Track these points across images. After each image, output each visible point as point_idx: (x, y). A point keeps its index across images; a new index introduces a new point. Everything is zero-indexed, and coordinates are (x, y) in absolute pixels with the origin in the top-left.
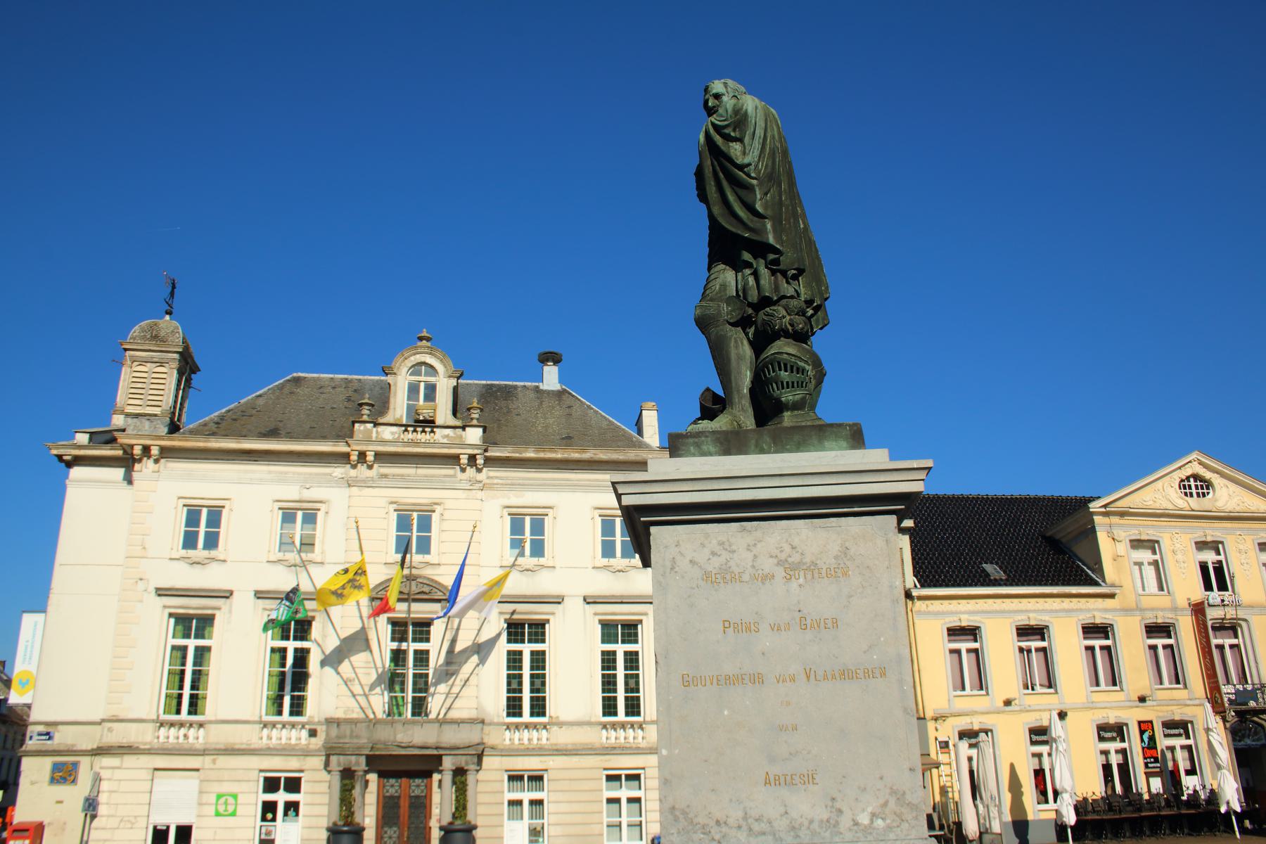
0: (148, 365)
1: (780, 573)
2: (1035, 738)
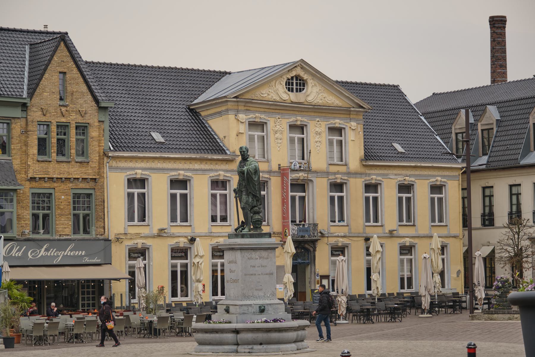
1: (259, 258)
2: (174, 254)
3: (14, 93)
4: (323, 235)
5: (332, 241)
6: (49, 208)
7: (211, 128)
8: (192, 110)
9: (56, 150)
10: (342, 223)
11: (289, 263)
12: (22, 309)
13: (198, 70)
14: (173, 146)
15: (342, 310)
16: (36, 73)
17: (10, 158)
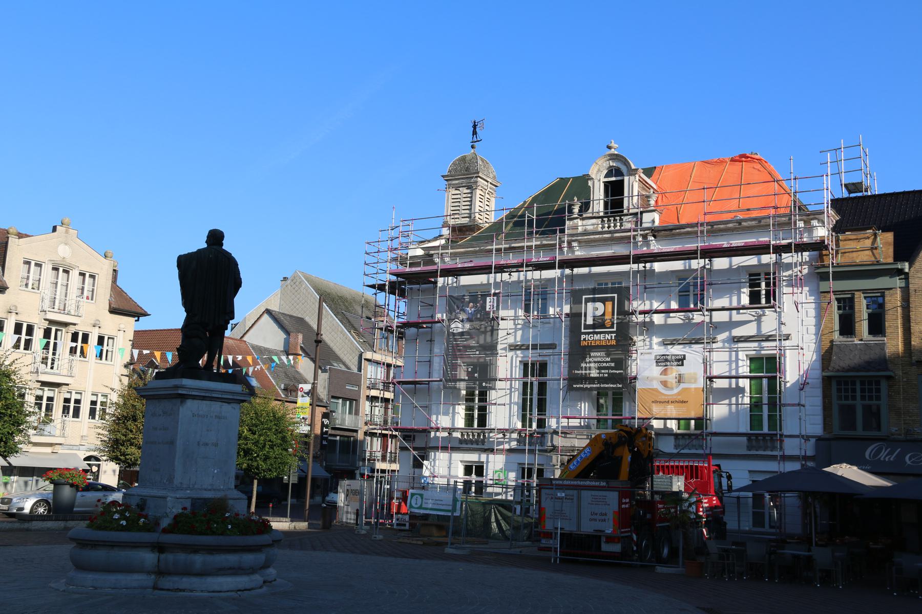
0: (460, 189)
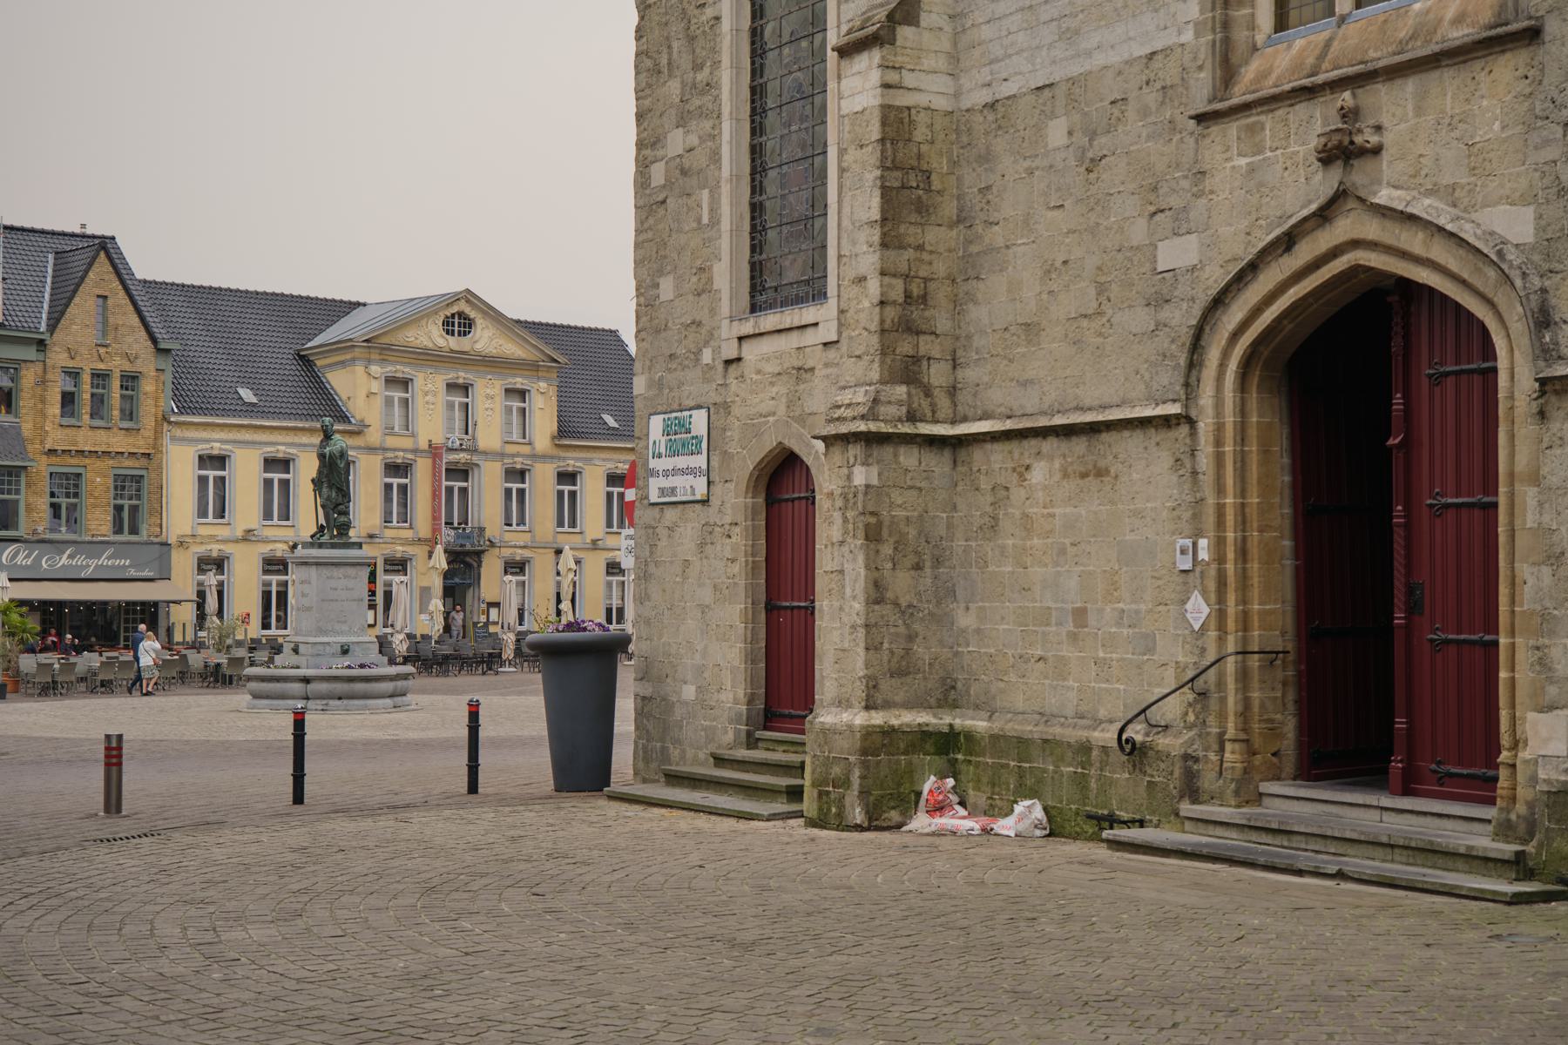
3: (25, 325)
4: (492, 544)
5: (506, 552)
6: (76, 495)
7: (330, 384)
8: (302, 357)
9: (89, 411)
10: (521, 528)
11: (437, 583)
12: (22, 641)
13: (317, 299)
14: (270, 410)
15: (508, 653)
16: (62, 296)
17: (18, 420)
